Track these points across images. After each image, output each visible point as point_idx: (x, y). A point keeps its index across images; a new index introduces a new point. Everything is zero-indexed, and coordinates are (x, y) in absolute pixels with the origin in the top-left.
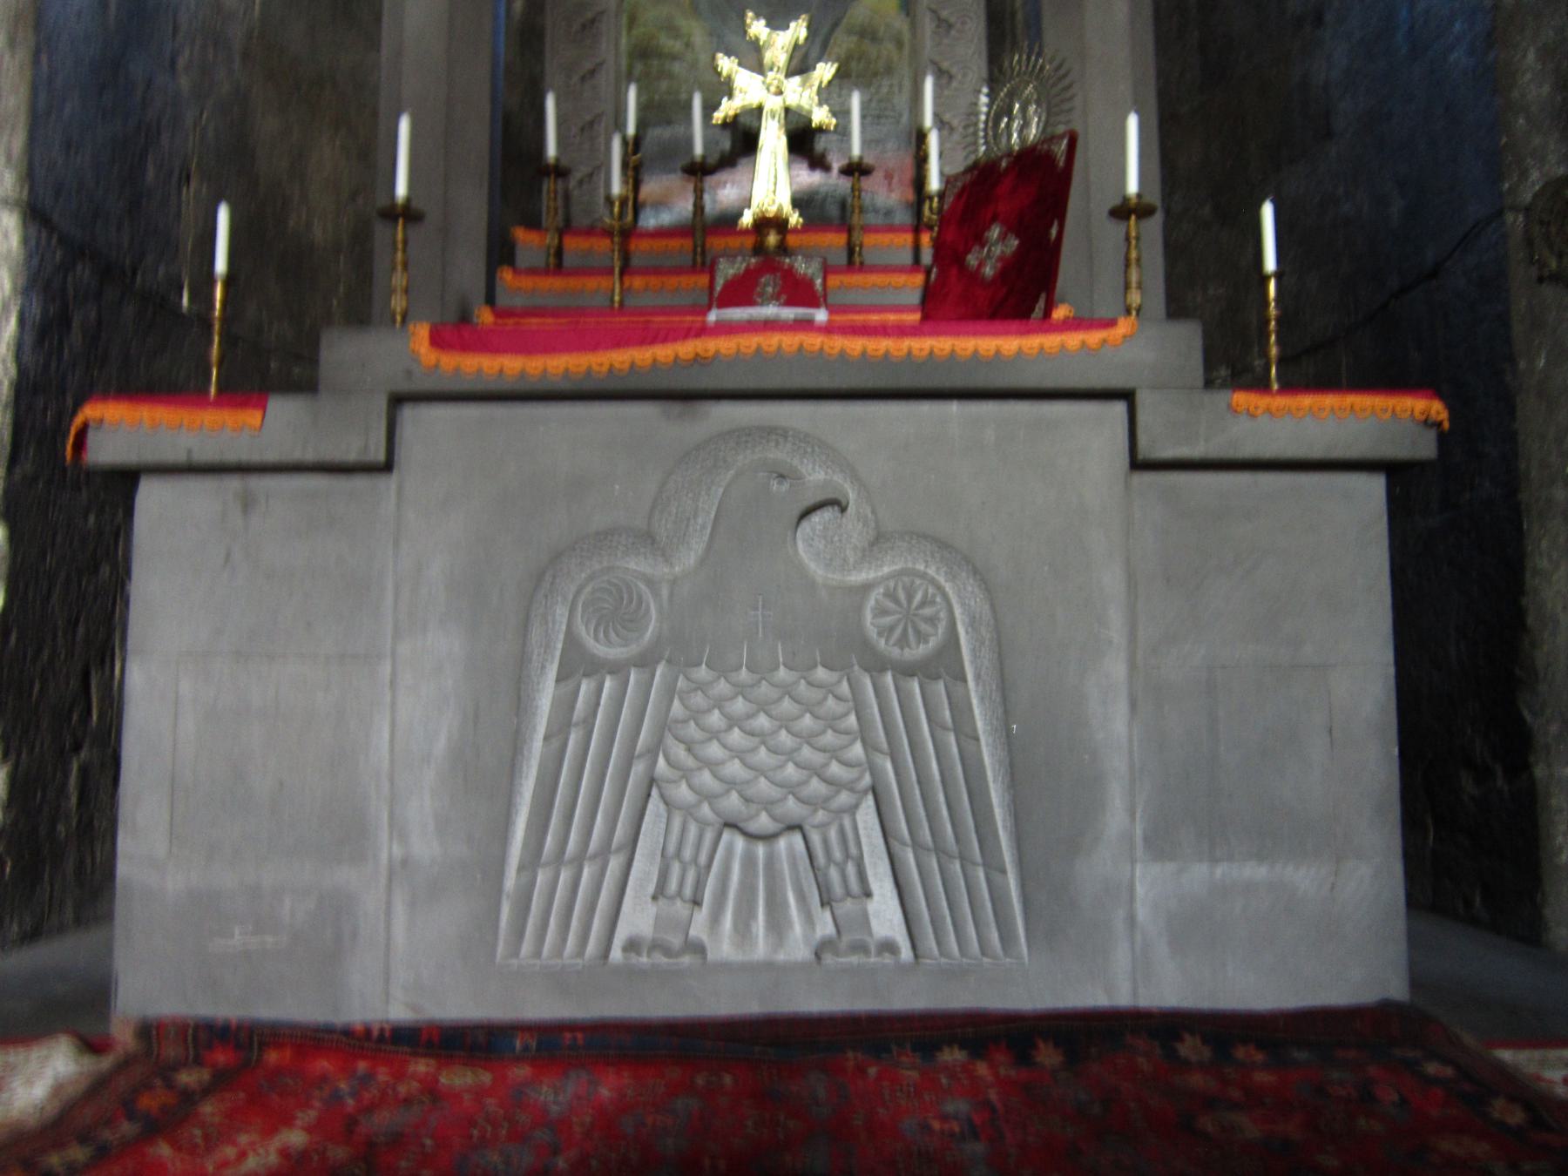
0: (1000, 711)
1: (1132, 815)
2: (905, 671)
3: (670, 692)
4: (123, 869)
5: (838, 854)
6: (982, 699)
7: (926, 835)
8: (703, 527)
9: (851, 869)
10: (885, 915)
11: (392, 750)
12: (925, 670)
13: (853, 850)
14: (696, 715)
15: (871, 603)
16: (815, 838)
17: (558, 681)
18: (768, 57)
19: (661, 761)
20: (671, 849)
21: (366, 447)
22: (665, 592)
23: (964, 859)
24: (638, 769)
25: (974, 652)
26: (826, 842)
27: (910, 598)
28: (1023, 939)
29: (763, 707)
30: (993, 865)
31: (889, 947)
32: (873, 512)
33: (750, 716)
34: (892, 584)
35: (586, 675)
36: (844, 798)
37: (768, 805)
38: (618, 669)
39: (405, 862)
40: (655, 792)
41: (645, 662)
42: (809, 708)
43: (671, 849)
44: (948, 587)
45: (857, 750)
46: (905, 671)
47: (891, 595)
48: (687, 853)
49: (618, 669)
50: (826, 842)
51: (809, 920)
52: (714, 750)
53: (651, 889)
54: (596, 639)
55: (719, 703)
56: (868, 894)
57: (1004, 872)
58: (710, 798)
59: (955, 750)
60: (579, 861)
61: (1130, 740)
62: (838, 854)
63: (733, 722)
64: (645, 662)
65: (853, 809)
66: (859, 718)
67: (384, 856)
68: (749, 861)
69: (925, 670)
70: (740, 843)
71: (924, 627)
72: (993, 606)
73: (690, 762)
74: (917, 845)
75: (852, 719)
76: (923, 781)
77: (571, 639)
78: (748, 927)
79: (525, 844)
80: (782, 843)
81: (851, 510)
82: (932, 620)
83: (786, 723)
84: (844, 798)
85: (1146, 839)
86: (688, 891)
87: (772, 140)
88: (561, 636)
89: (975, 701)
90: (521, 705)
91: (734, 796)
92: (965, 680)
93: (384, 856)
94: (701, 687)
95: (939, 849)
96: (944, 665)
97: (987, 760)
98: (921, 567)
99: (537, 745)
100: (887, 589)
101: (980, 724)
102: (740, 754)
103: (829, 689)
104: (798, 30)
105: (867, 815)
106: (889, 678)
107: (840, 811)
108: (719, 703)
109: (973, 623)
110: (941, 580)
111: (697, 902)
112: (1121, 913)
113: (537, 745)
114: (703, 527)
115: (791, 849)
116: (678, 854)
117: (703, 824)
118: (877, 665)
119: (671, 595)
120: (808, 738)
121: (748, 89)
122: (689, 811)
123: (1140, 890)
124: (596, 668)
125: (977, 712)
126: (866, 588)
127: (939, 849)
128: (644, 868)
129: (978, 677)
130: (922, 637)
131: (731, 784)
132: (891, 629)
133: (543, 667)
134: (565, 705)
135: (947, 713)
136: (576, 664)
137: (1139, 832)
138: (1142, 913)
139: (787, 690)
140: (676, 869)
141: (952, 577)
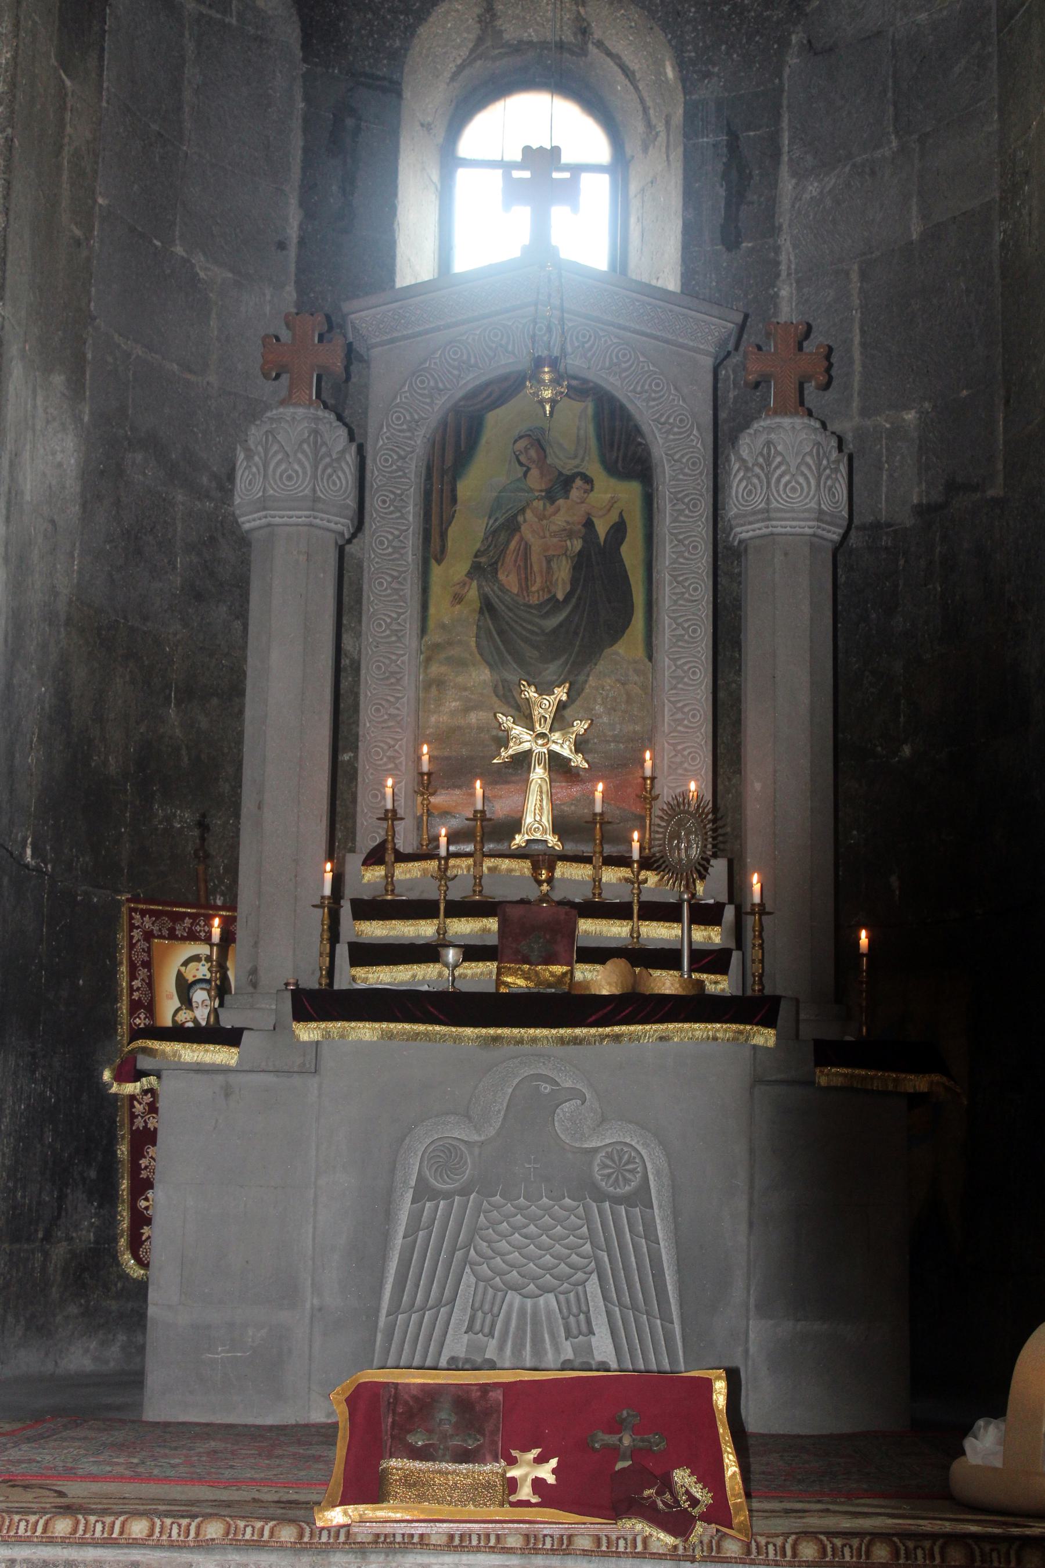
0: (672, 1227)
1: (748, 1291)
2: (616, 1200)
3: (478, 1210)
4: (152, 1311)
5: (575, 1310)
6: (662, 1220)
7: (627, 1300)
8: (499, 1111)
9: (582, 1317)
10: (603, 1348)
11: (314, 1239)
12: (627, 1200)
13: (584, 1308)
14: (493, 1224)
15: (597, 1161)
16: (562, 1297)
17: (414, 1201)
18: (537, 712)
19: (472, 1251)
20: (477, 1305)
21: (304, 1064)
22: (476, 1151)
23: (648, 1313)
24: (459, 1254)
25: (659, 1192)
26: (568, 1301)
27: (620, 1159)
28: (682, 1360)
29: (533, 1219)
30: (666, 1317)
31: (604, 1367)
32: (601, 1108)
33: (526, 1226)
34: (610, 1150)
35: (428, 1200)
36: (580, 1275)
37: (534, 1279)
38: (448, 1195)
39: (320, 1310)
40: (468, 1269)
41: (465, 1192)
42: (559, 1221)
43: (477, 1305)
44: (643, 1152)
45: (588, 1247)
46: (616, 1200)
47: (609, 1156)
48: (487, 1307)
49: (448, 1195)
50: (568, 1301)
51: (557, 1349)
52: (503, 1245)
53: (464, 1329)
54: (435, 1179)
55: (507, 1217)
56: (591, 1332)
57: (673, 1323)
58: (502, 1274)
59: (645, 1250)
60: (423, 1309)
61: (749, 1246)
62: (575, 1310)
63: (515, 1229)
64: (465, 1192)
65: (583, 1283)
66: (588, 1228)
67: (308, 1306)
68: (522, 1313)
69: (627, 1200)
70: (517, 1300)
71: (628, 1176)
72: (669, 1165)
73: (490, 1253)
74: (621, 1304)
75: (585, 1229)
76: (626, 1268)
77: (421, 1178)
78: (520, 1351)
79: (391, 1298)
80: (541, 1300)
81: (587, 1103)
82: (633, 1171)
83: (546, 1230)
84: (580, 1275)
85: (756, 1306)
86: (486, 1330)
87: (539, 774)
88: (414, 1177)
89: (658, 1221)
90: (389, 1215)
91: (514, 1272)
92: (652, 1207)
93: (308, 1306)
94: (497, 1207)
95: (635, 1308)
96: (641, 1197)
97: (664, 1257)
98: (628, 1140)
99: (398, 1241)
100: (607, 1153)
101: (660, 1235)
102: (519, 1248)
103: (571, 1210)
104: (561, 693)
105: (593, 1286)
106: (607, 1205)
107: (576, 1285)
108: (507, 1217)
109: (658, 1173)
110: (639, 1148)
111: (491, 1334)
112: (740, 1349)
113: (398, 1241)
114: (499, 1111)
115: (547, 1304)
116: (481, 1307)
117: (496, 1289)
118: (600, 1196)
119: (480, 1154)
120: (559, 1239)
121: (522, 739)
122: (487, 1280)
123: (752, 1335)
124: (435, 1195)
125: (659, 1227)
126: (596, 1150)
127: (635, 1308)
128: (460, 1315)
129: (660, 1206)
130: (627, 1181)
131: (513, 1266)
132: (609, 1175)
133: (402, 1195)
134: (415, 1218)
135: (641, 1228)
136: (423, 1192)
137: (752, 1301)
138: (752, 1350)
139: (547, 1210)
140: (480, 1314)
141: (646, 1145)
